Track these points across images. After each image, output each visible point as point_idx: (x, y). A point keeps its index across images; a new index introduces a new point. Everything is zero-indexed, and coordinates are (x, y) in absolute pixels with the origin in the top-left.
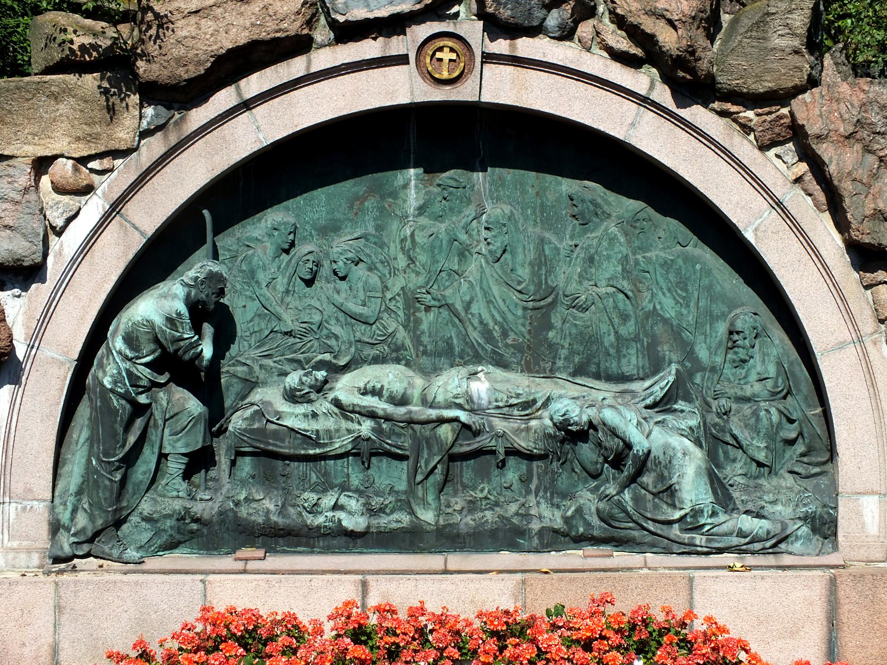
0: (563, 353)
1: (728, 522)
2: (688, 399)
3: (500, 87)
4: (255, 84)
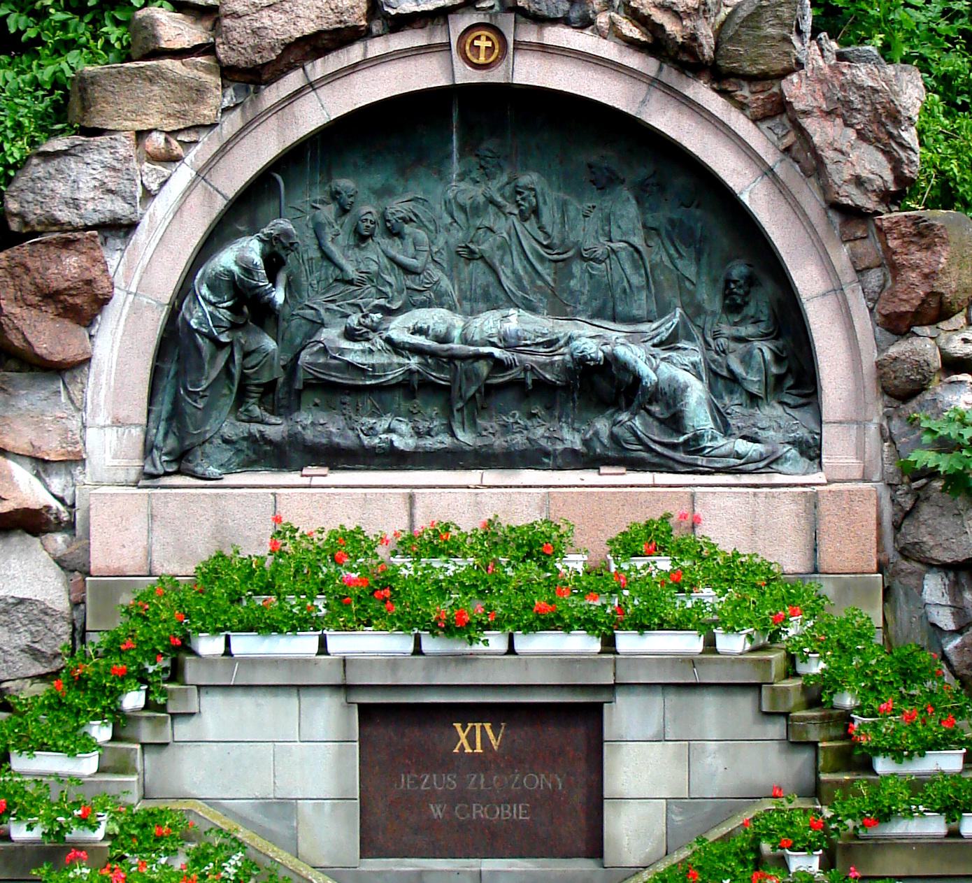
0: (584, 298)
1: (724, 444)
2: (690, 338)
3: (528, 72)
4: (319, 68)
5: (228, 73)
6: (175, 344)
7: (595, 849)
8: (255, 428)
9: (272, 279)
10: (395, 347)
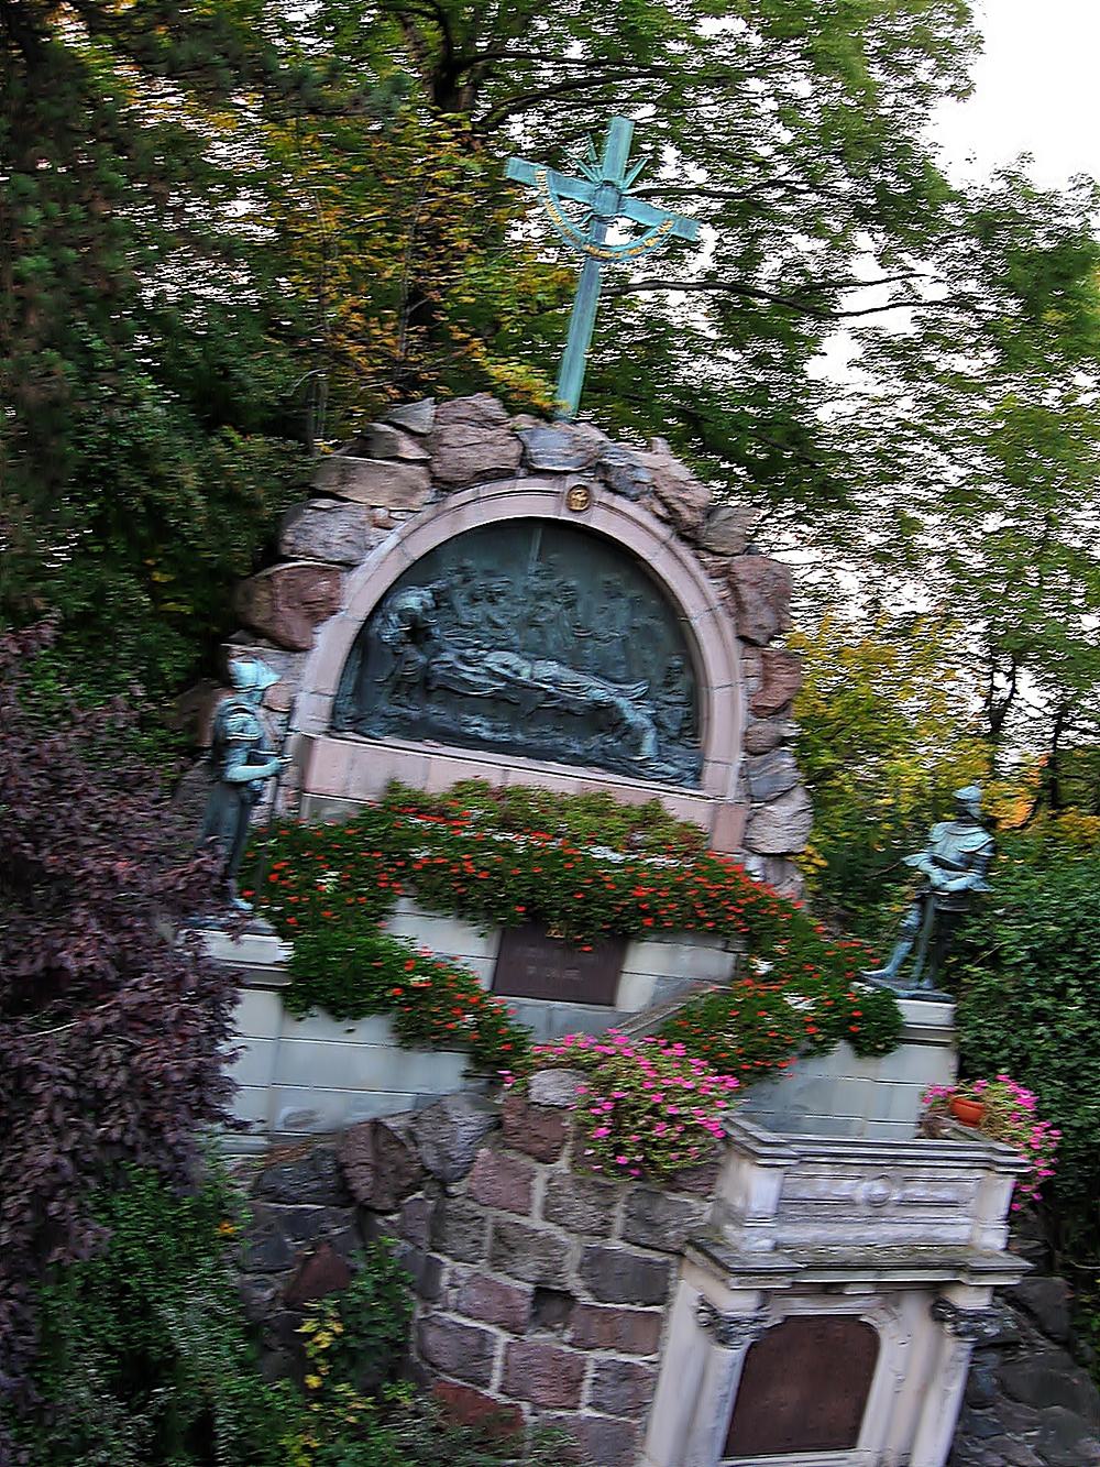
3: (598, 520)
4: (486, 489)
5: (434, 479)
6: (363, 644)
10: (492, 674)
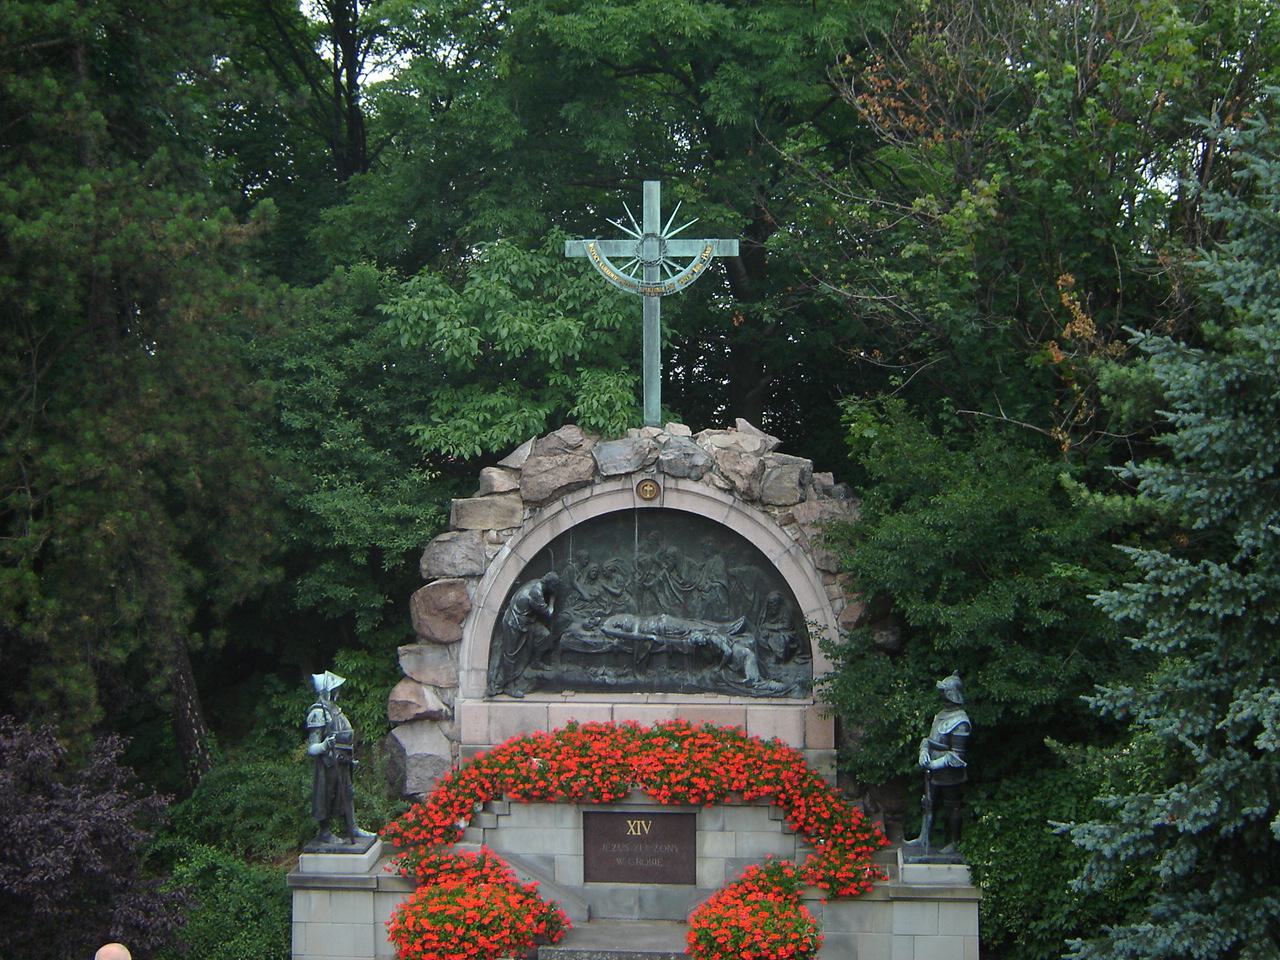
3: (672, 502)
4: (570, 499)
5: (525, 502)
7: (693, 881)
8: (540, 673)
9: (547, 601)
10: (607, 634)
